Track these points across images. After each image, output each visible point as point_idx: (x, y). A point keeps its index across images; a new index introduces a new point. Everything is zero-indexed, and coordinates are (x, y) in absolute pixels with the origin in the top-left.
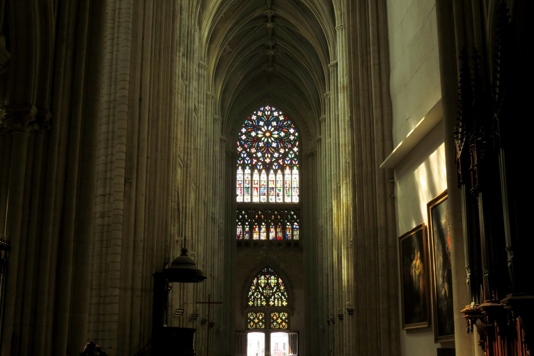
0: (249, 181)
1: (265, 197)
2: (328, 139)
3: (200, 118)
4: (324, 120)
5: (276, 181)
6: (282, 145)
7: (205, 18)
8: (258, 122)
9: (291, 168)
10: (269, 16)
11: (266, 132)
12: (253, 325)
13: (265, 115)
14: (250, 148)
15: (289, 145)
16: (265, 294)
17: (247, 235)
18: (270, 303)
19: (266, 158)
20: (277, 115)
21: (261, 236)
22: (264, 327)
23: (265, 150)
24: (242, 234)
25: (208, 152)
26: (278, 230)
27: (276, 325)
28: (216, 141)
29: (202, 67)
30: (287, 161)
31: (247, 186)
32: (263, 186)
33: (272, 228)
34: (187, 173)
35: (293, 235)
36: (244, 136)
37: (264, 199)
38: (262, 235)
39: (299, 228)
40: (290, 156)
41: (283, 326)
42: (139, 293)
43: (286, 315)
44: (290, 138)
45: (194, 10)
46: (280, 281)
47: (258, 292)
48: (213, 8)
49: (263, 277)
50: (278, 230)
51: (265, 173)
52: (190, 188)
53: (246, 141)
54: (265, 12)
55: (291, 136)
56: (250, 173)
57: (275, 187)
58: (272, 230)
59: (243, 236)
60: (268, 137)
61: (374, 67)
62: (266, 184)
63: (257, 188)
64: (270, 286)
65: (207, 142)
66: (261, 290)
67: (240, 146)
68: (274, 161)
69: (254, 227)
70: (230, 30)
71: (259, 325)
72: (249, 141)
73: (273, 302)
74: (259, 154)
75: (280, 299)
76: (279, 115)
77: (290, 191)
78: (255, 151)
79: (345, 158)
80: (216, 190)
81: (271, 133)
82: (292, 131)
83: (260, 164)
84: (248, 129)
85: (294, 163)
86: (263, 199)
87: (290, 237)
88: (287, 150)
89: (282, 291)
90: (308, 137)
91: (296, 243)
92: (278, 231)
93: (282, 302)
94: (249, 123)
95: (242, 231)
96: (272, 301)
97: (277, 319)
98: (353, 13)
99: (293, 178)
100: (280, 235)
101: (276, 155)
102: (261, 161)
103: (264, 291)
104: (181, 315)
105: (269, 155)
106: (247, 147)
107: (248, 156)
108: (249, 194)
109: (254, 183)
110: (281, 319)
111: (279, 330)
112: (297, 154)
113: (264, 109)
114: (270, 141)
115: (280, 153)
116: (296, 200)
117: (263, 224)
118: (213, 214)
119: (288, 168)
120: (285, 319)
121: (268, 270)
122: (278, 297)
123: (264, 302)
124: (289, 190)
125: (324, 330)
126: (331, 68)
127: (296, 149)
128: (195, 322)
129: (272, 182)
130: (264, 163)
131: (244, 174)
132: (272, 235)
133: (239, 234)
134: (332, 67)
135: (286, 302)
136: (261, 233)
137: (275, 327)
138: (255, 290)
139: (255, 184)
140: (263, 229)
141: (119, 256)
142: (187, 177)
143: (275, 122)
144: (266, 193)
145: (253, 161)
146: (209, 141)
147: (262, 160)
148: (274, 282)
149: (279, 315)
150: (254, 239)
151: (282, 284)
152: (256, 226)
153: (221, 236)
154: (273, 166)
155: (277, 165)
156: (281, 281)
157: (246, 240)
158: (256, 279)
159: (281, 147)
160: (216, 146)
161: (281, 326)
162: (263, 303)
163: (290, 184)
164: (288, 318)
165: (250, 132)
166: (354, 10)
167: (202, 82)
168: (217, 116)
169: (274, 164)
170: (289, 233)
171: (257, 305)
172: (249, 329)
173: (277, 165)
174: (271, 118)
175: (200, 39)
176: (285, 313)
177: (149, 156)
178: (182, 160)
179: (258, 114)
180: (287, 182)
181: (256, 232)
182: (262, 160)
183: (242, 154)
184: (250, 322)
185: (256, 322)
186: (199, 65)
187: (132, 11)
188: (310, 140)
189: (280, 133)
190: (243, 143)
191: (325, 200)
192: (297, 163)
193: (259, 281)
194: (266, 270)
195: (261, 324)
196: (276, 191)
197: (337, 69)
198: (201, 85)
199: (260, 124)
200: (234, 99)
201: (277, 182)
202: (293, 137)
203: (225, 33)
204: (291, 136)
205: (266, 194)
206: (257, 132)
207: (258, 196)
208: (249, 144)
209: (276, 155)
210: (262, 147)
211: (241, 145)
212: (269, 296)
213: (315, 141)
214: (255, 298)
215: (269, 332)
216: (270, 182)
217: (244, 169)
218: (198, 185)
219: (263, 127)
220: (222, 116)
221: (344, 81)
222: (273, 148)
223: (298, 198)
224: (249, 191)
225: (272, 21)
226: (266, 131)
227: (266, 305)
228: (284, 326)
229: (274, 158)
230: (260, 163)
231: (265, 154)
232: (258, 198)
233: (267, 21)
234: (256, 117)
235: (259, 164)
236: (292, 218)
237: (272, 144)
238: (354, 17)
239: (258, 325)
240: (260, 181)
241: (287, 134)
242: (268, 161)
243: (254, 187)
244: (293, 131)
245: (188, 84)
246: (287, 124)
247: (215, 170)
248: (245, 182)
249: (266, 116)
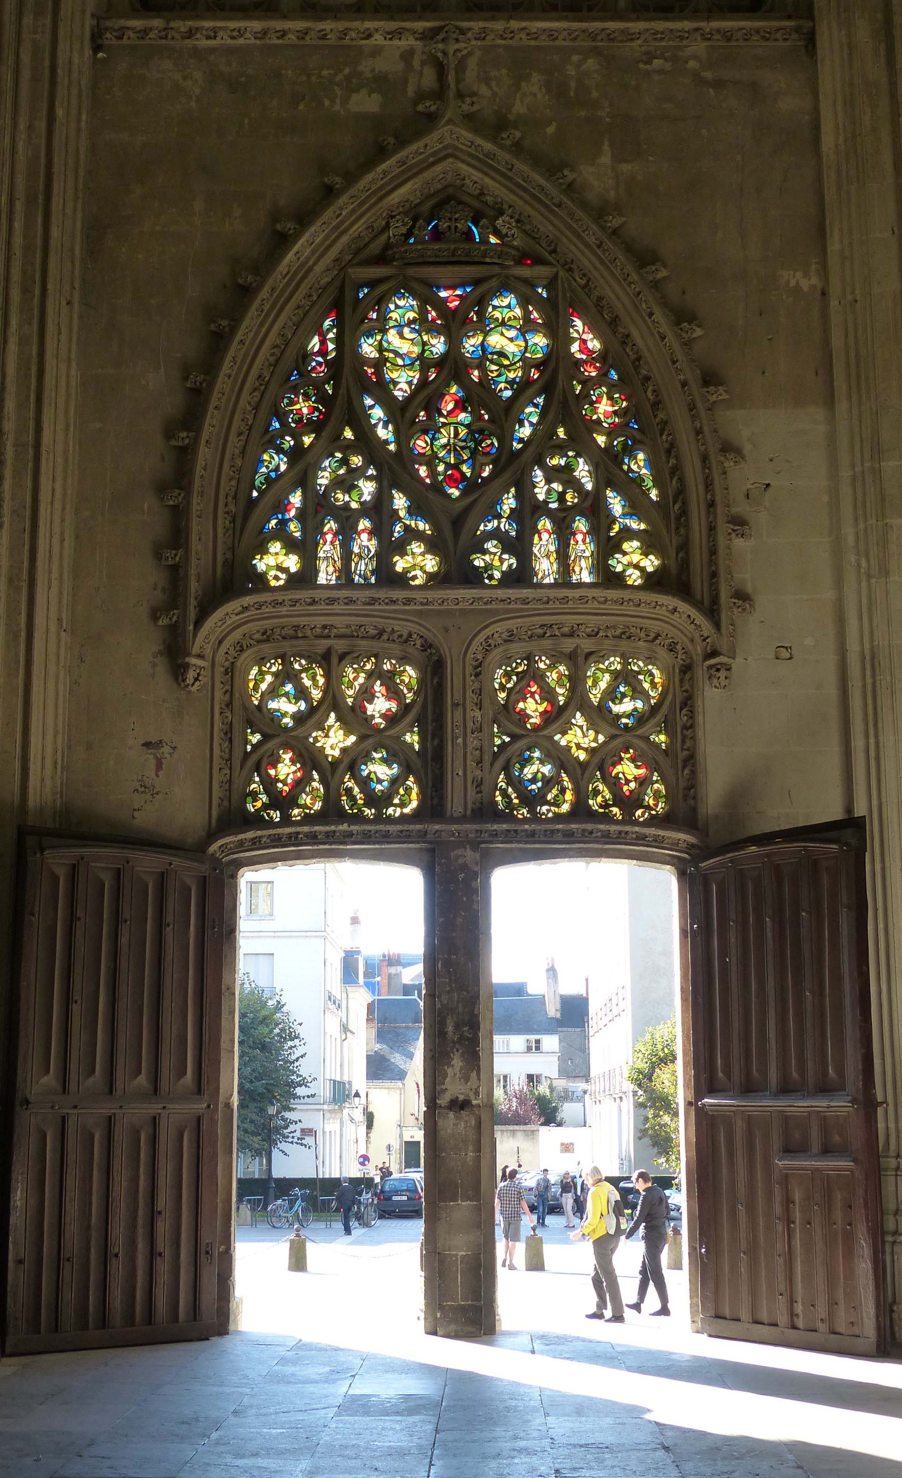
12: (300, 785)
16: (423, 471)
22: (414, 804)
41: (619, 799)
47: (349, 448)
71: (365, 783)
73: (508, 545)
75: (581, 525)
89: (601, 440)
96: (495, 534)
122: (561, 497)
123: (417, 547)
137: (531, 800)
149: (576, 681)
151: (603, 374)
156: (594, 344)
162: (400, 564)
172: (256, 821)
215: (469, 856)
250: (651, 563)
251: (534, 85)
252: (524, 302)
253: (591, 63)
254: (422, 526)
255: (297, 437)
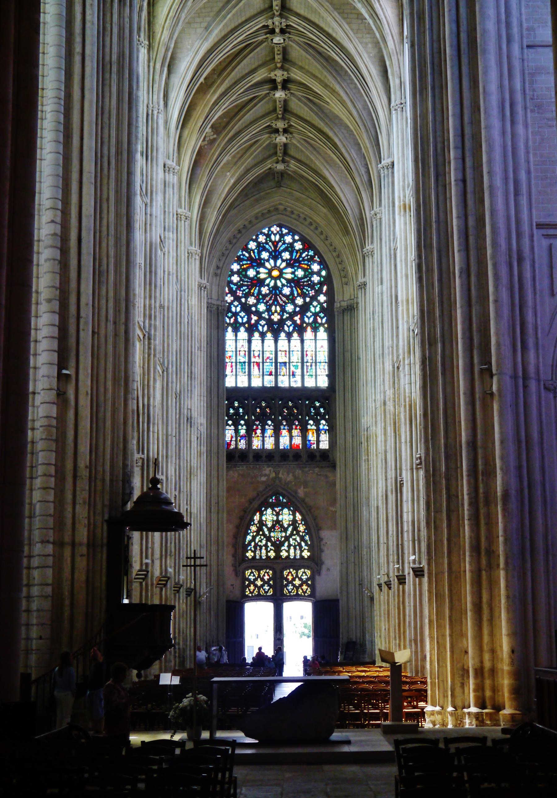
0: (245, 351)
1: (272, 378)
2: (378, 286)
3: (168, 255)
4: (370, 253)
5: (289, 352)
6: (300, 291)
7: (173, 86)
8: (259, 253)
9: (315, 330)
10: (279, 79)
11: (273, 270)
12: (254, 590)
13: (271, 241)
14: (247, 296)
15: (310, 292)
16: (273, 539)
17: (242, 441)
18: (282, 554)
19: (273, 314)
20: (291, 241)
21: (265, 443)
23: (270, 299)
24: (234, 439)
25: (181, 310)
26: (295, 432)
27: (292, 589)
28: (192, 290)
29: (169, 171)
30: (309, 318)
31: (242, 360)
32: (268, 361)
33: (284, 429)
34: (149, 348)
35: (318, 441)
36: (236, 276)
37: (271, 381)
38: (267, 441)
39: (328, 430)
40: (312, 309)
41: (303, 592)
42: (84, 550)
43: (308, 572)
44: (312, 279)
45: (157, 77)
46: (298, 517)
47: (261, 535)
48: (187, 70)
49: (269, 511)
50: (295, 432)
51: (272, 338)
52: (154, 372)
53: (239, 287)
54: (272, 75)
55: (315, 276)
56: (247, 338)
57: (287, 361)
58: (285, 433)
59: (236, 444)
60: (276, 279)
61: (456, 185)
62: (273, 356)
63: (258, 364)
64: (282, 526)
65: (179, 293)
66: (267, 533)
67: (228, 293)
68: (287, 319)
69: (255, 427)
70: (216, 103)
71: (264, 590)
72: (245, 285)
73: (287, 551)
74: (262, 307)
75: (298, 547)
76: (295, 241)
77: (314, 367)
78: (255, 301)
79: (408, 322)
80: (193, 371)
81: (281, 271)
82: (315, 267)
83: (262, 324)
84: (243, 265)
85: (319, 320)
86: (269, 382)
87: (314, 444)
88: (308, 300)
89: (301, 534)
90: (343, 279)
91: (324, 455)
92: (293, 434)
93: (302, 551)
94: (244, 255)
95: (234, 435)
96: (284, 549)
97: (294, 579)
98: (421, 94)
99: (317, 347)
100: (298, 441)
101: (290, 308)
102: (264, 319)
103: (272, 534)
104: (143, 579)
105: (278, 309)
106: (241, 295)
107: (242, 309)
108: (245, 372)
109: (254, 356)
110: (300, 579)
111: (297, 597)
112: (325, 306)
113: (268, 231)
114: (279, 284)
115: (296, 306)
116: (323, 382)
117: (269, 422)
118: (189, 411)
119: (309, 329)
120: (306, 579)
121: (277, 499)
123: (272, 552)
124: (311, 366)
125: (372, 599)
126: (384, 170)
127: (322, 298)
128: (164, 589)
129: (283, 353)
130: (270, 322)
131: (236, 340)
132: (284, 442)
133: (230, 439)
134: (385, 170)
135: (308, 552)
136: (265, 439)
137: (290, 592)
138: (258, 532)
139: (255, 357)
140: (269, 432)
141: (52, 492)
142: (149, 355)
143: (287, 253)
144: (273, 371)
145: (252, 319)
146: (181, 291)
147: (267, 317)
148: (287, 519)
149: (297, 573)
150: (254, 447)
152: (257, 426)
153: (200, 446)
154: (285, 326)
155: (291, 325)
156: (300, 517)
157: (241, 449)
158: (258, 514)
159: (298, 295)
160: (191, 297)
161: (300, 592)
162: (269, 554)
163: (314, 356)
164: (312, 578)
165: (246, 270)
166: (423, 88)
167: (169, 195)
168: (193, 248)
169: (287, 323)
170: (312, 437)
171: (261, 556)
172: (247, 596)
173: (291, 325)
174: (281, 246)
175: (166, 122)
176: (306, 570)
177: (96, 330)
178: (142, 327)
179: (259, 240)
180: (308, 353)
181: (258, 436)
182: (267, 317)
183: (232, 306)
184: (249, 586)
185: (259, 585)
186: (164, 166)
187: (63, 93)
188: (346, 284)
189: (295, 271)
190: (234, 288)
191: (373, 385)
192: (324, 320)
193: (264, 518)
194: (275, 500)
195: (266, 587)
196: (289, 368)
197: (393, 173)
198: (169, 200)
199: (262, 257)
200: (220, 217)
201: (291, 352)
202: (318, 278)
203: (207, 110)
204: (315, 276)
205: (273, 373)
206: (258, 270)
207: (259, 377)
208: (244, 290)
209: (290, 308)
210: (265, 296)
211: (233, 293)
212: (280, 541)
213: (356, 286)
214: (256, 545)
215: (280, 602)
216: (279, 353)
217: (236, 330)
218: (166, 365)
219: (268, 261)
220: (201, 246)
221: (405, 196)
222: (284, 296)
223: (326, 379)
224: (245, 369)
225: (284, 88)
226: (272, 267)
227: (275, 558)
228: (305, 590)
229: (287, 313)
230: (263, 322)
231: (271, 306)
232: (261, 379)
233: (275, 88)
234: (255, 244)
235: (260, 322)
236: (318, 413)
237: (282, 288)
238: (424, 101)
239: (261, 589)
240: (263, 352)
241: (307, 273)
242: (276, 318)
243: (254, 362)
244: (318, 267)
245: (149, 201)
246: (307, 255)
247: (192, 337)
248: (238, 353)
249: (273, 243)
250: (309, 554)
251: (291, 475)
252: (289, 510)
253: (300, 472)
254: (273, 548)
255: (253, 533)
